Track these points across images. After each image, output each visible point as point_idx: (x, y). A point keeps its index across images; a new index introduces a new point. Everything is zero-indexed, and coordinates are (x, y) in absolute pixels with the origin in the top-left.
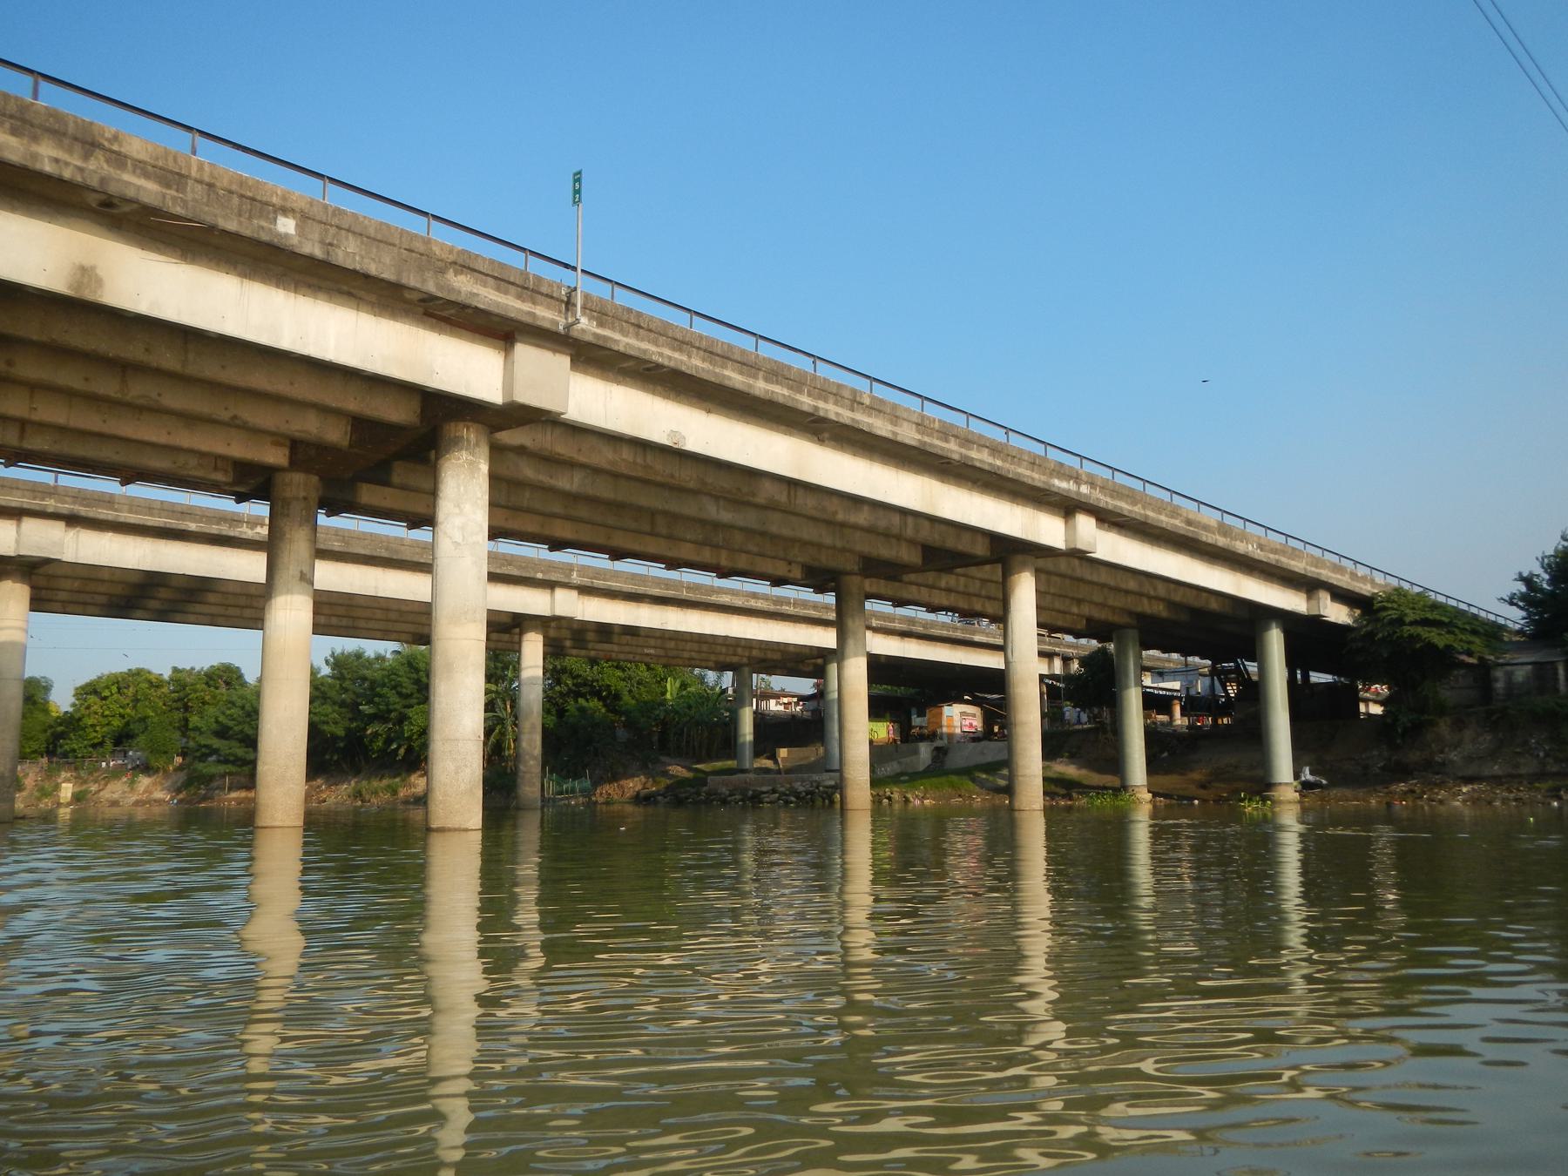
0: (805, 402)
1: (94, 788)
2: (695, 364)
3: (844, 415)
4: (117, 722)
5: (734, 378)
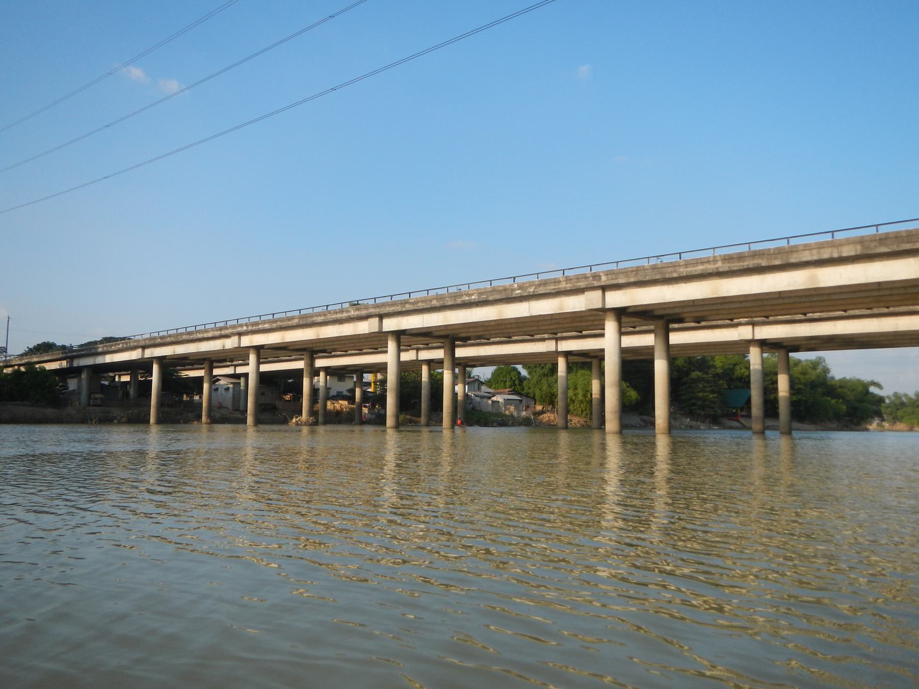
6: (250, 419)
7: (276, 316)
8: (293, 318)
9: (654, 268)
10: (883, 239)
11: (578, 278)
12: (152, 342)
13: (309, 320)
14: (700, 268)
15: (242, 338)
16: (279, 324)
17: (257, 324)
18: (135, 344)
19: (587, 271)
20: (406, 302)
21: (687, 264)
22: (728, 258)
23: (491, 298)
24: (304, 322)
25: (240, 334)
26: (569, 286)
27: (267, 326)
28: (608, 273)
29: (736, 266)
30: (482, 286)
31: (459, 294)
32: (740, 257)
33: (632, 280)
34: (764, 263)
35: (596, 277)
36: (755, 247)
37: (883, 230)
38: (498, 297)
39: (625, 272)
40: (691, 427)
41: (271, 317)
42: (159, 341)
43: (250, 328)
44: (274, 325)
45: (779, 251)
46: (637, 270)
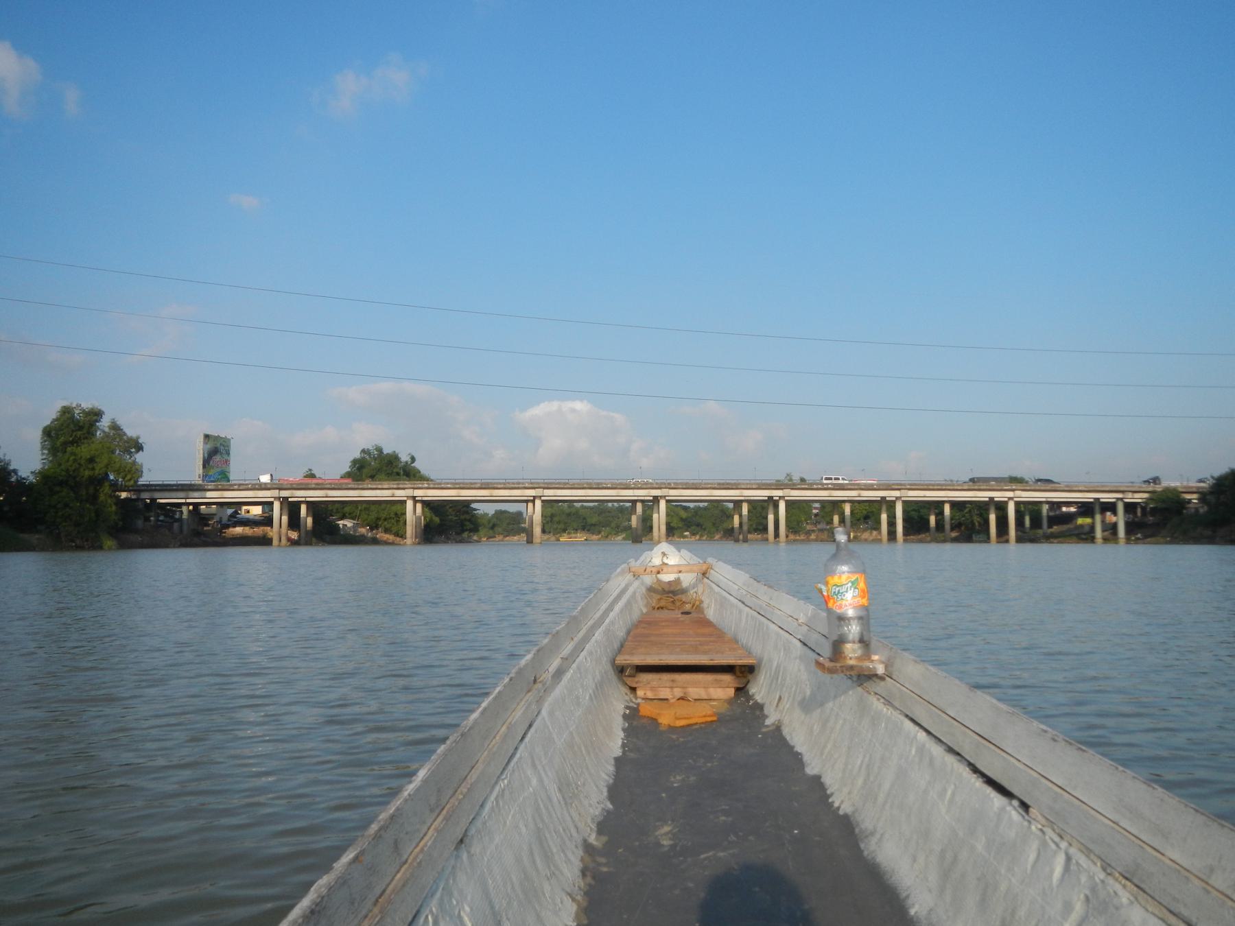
0: (944, 487)
1: (859, 534)
2: (925, 487)
3: (951, 488)
4: (865, 512)
5: (931, 487)
6: (409, 541)
7: (457, 481)
8: (475, 483)
9: (693, 484)
10: (764, 484)
11: (662, 483)
12: (303, 487)
13: (490, 486)
14: (709, 486)
15: (415, 491)
16: (461, 486)
17: (440, 484)
18: (274, 486)
19: (665, 481)
20: (568, 483)
21: (705, 484)
22: (719, 484)
23: (619, 487)
24: (487, 487)
25: (414, 488)
26: (657, 486)
27: (449, 486)
28: (674, 483)
29: (722, 487)
30: (613, 481)
31: (598, 484)
32: (723, 484)
33: (684, 487)
34: (730, 487)
35: (669, 484)
36: (728, 481)
37: (764, 482)
38: (622, 487)
39: (681, 484)
40: (445, 542)
41: (454, 481)
42: (313, 486)
43: (432, 486)
44: (458, 486)
45: (735, 484)
46: (687, 484)
